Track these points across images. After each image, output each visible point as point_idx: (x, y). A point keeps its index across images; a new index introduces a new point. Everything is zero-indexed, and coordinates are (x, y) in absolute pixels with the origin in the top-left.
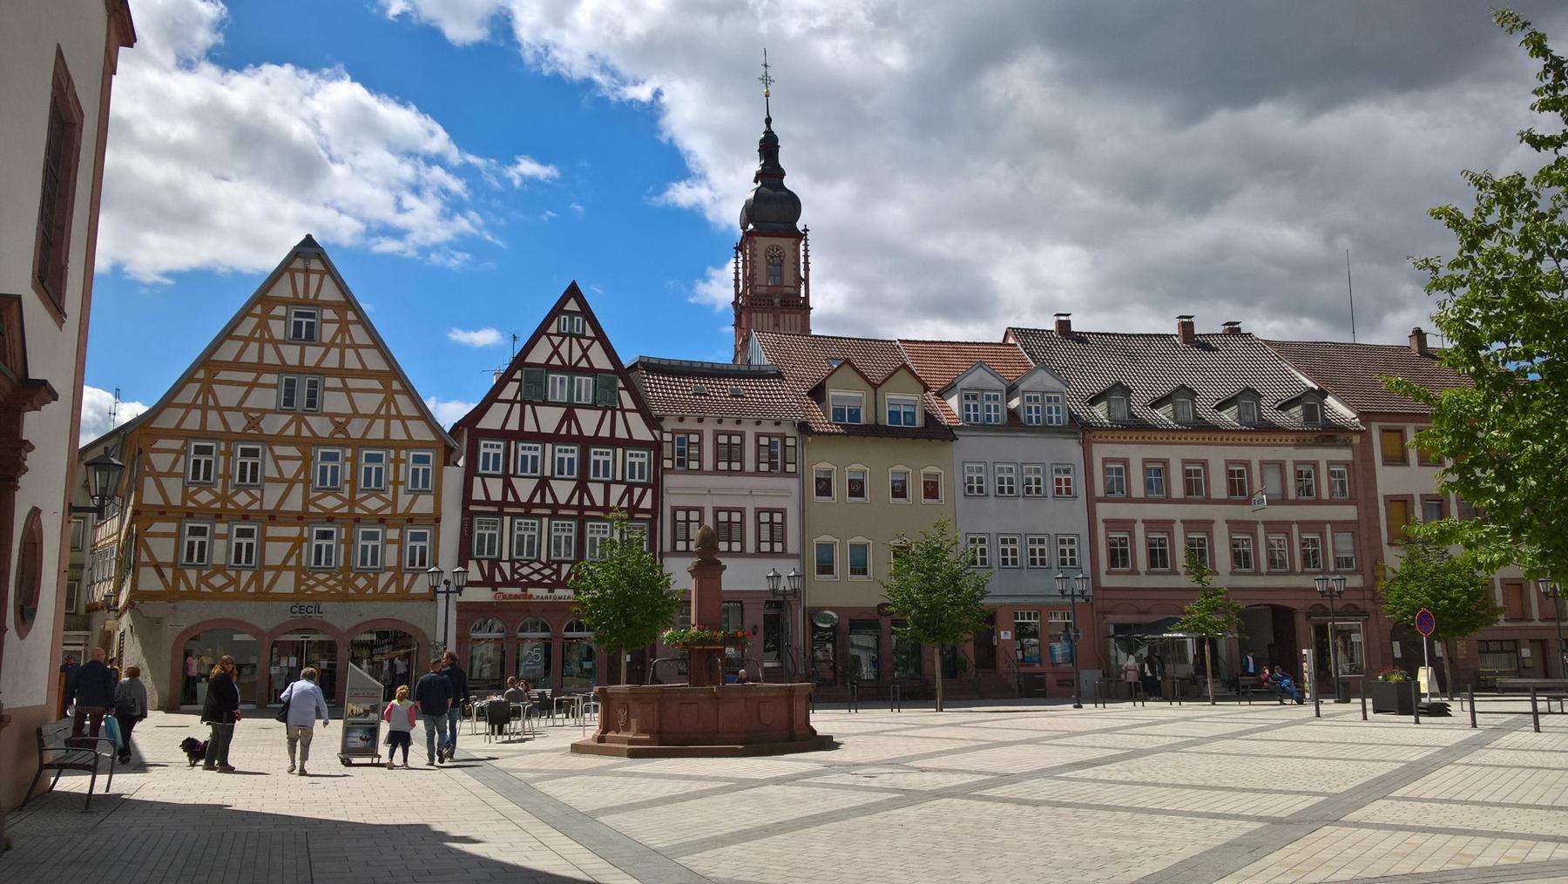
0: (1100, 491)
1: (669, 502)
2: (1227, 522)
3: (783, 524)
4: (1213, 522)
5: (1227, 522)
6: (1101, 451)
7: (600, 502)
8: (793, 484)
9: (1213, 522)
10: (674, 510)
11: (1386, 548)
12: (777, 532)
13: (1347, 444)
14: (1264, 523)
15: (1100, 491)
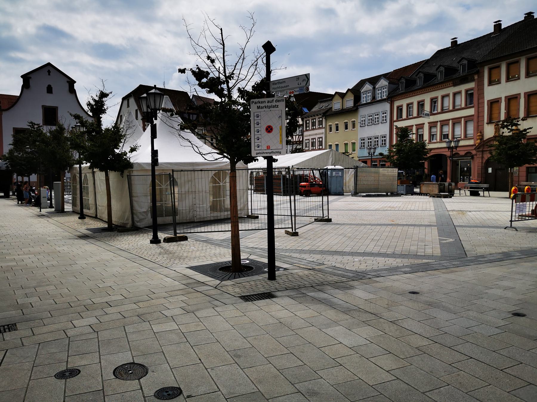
0: (395, 119)
1: (305, 138)
2: (429, 123)
3: (322, 141)
4: (424, 124)
5: (429, 123)
6: (397, 104)
7: (295, 141)
8: (323, 131)
9: (424, 124)
10: (306, 140)
11: (485, 125)
12: (321, 143)
13: (472, 80)
14: (440, 121)
15: (395, 119)
